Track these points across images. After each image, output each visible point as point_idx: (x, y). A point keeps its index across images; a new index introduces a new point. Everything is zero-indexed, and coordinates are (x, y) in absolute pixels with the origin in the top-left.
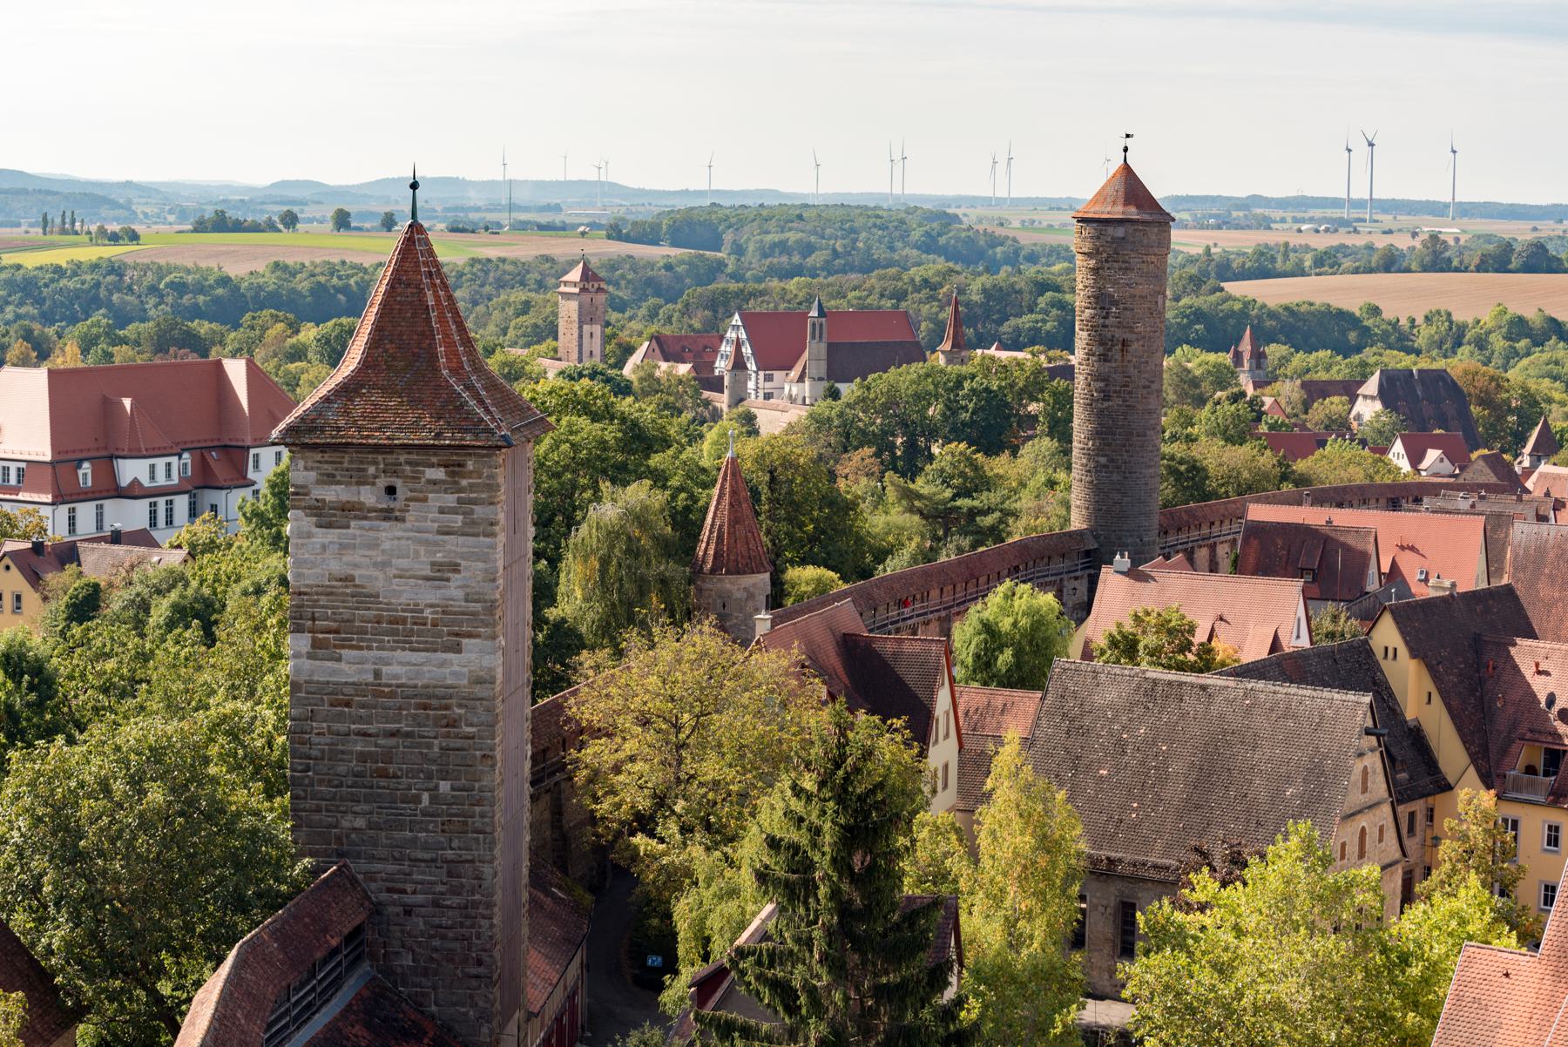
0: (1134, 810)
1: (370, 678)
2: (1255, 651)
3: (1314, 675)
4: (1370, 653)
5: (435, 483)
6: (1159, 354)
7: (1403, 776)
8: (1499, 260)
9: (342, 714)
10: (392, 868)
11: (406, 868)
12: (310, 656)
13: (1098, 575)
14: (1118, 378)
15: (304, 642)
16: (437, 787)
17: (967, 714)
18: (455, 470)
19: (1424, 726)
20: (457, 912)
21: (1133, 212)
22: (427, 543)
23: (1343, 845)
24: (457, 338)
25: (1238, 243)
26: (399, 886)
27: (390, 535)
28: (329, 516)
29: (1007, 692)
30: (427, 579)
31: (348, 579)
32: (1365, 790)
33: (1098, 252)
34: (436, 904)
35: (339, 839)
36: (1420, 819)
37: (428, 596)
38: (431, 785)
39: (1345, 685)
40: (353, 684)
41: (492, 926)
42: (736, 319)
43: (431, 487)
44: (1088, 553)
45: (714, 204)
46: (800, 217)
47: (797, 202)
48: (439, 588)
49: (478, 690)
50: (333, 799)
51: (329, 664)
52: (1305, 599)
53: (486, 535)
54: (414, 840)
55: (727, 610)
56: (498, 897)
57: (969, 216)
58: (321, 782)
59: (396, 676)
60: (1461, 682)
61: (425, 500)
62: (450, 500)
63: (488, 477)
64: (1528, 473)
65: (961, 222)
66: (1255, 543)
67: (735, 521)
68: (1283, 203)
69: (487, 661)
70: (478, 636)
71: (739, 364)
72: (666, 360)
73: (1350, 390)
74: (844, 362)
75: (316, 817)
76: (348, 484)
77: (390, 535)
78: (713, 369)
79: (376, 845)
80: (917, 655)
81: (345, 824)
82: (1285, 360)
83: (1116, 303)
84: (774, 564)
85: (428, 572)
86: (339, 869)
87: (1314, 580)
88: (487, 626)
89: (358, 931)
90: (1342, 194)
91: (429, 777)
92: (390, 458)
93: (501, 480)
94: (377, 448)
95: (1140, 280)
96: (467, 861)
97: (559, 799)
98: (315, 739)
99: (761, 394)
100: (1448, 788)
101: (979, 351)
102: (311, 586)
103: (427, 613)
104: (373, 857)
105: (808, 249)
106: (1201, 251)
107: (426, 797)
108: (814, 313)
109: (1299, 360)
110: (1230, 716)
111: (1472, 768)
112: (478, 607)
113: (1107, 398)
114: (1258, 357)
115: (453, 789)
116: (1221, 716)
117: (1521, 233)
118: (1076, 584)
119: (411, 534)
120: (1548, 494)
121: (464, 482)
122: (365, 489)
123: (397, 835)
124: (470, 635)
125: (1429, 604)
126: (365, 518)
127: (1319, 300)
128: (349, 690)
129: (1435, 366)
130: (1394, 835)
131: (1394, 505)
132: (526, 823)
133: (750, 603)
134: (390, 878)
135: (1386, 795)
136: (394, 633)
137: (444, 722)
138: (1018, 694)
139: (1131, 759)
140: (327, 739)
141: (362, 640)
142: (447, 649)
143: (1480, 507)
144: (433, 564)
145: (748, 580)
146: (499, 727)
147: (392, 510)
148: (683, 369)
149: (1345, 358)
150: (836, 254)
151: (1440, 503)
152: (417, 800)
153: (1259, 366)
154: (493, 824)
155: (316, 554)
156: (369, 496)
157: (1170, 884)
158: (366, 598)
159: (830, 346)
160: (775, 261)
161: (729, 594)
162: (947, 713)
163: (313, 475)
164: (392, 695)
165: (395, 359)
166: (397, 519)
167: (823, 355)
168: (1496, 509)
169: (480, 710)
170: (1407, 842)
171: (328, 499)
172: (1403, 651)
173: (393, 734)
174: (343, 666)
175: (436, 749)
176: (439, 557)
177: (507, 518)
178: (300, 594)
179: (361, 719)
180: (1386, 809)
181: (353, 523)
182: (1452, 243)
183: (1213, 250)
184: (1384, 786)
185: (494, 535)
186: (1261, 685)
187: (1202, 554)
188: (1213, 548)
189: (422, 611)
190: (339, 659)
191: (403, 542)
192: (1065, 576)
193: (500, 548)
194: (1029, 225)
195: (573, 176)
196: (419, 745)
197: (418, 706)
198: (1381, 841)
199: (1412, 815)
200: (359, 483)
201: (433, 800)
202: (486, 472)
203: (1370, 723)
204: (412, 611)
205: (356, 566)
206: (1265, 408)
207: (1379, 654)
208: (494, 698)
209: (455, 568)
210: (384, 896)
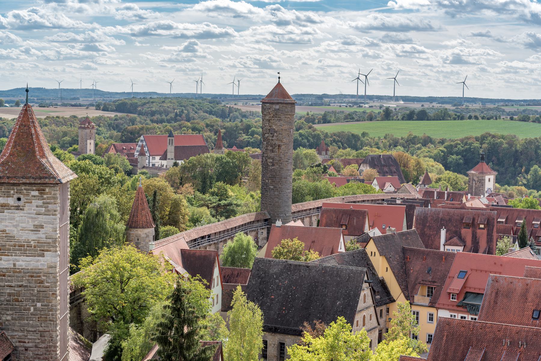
0: (284, 310)
1: (12, 266)
3: (347, 262)
7: (378, 297)
8: (410, 116)
10: (20, 334)
11: (25, 334)
13: (270, 228)
14: (277, 158)
16: (36, 305)
17: (224, 277)
18: (42, 192)
22: (32, 218)
25: (318, 111)
26: (23, 340)
27: (19, 215)
30: (32, 231)
32: (365, 302)
33: (270, 114)
36: (384, 312)
37: (32, 237)
38: (34, 304)
40: (6, 268)
41: (57, 354)
43: (33, 198)
44: (266, 220)
49: (51, 271)
53: (53, 215)
54: (28, 324)
55: (139, 241)
59: (21, 266)
61: (31, 203)
62: (40, 202)
63: (54, 194)
69: (53, 260)
70: (50, 251)
71: (142, 154)
74: (181, 152)
76: (4, 197)
77: (19, 215)
81: (4, 318)
83: (276, 132)
85: (32, 228)
88: (54, 247)
89: (9, 356)
91: (33, 301)
92: (19, 188)
93: (58, 196)
94: (14, 184)
95: (285, 124)
96: (47, 331)
97: (80, 309)
100: (394, 301)
103: (32, 243)
104: (14, 330)
105: (167, 113)
107: (32, 308)
109: (341, 151)
112: (50, 241)
113: (273, 165)
115: (42, 306)
116: (314, 276)
118: (263, 231)
119: (26, 215)
121: (45, 196)
123: (22, 322)
124: (47, 251)
126: (10, 209)
128: (4, 271)
130: (375, 318)
132: (68, 317)
133: (147, 239)
134: (20, 337)
135: (372, 303)
136: (20, 250)
137: (39, 282)
141: (9, 253)
142: (39, 256)
144: (34, 225)
145: (146, 231)
147: (19, 206)
152: (29, 309)
156: (11, 201)
158: (10, 238)
159: (175, 147)
161: (140, 235)
164: (20, 272)
165: (20, 152)
166: (21, 209)
167: (173, 150)
169: (51, 277)
170: (380, 320)
172: (377, 254)
173: (20, 286)
175: (36, 292)
176: (36, 223)
177: (60, 209)
179: (9, 281)
180: (372, 309)
181: (5, 211)
182: (394, 111)
184: (372, 300)
185: (56, 215)
188: (310, 217)
189: (30, 242)
191: (23, 218)
192: (259, 228)
195: (84, 87)
197: (29, 276)
198: (370, 320)
199: (381, 311)
200: (7, 197)
201: (35, 309)
202: (53, 192)
204: (26, 242)
205: (7, 226)
207: (369, 254)
208: (56, 273)
209: (42, 227)
210: (18, 344)
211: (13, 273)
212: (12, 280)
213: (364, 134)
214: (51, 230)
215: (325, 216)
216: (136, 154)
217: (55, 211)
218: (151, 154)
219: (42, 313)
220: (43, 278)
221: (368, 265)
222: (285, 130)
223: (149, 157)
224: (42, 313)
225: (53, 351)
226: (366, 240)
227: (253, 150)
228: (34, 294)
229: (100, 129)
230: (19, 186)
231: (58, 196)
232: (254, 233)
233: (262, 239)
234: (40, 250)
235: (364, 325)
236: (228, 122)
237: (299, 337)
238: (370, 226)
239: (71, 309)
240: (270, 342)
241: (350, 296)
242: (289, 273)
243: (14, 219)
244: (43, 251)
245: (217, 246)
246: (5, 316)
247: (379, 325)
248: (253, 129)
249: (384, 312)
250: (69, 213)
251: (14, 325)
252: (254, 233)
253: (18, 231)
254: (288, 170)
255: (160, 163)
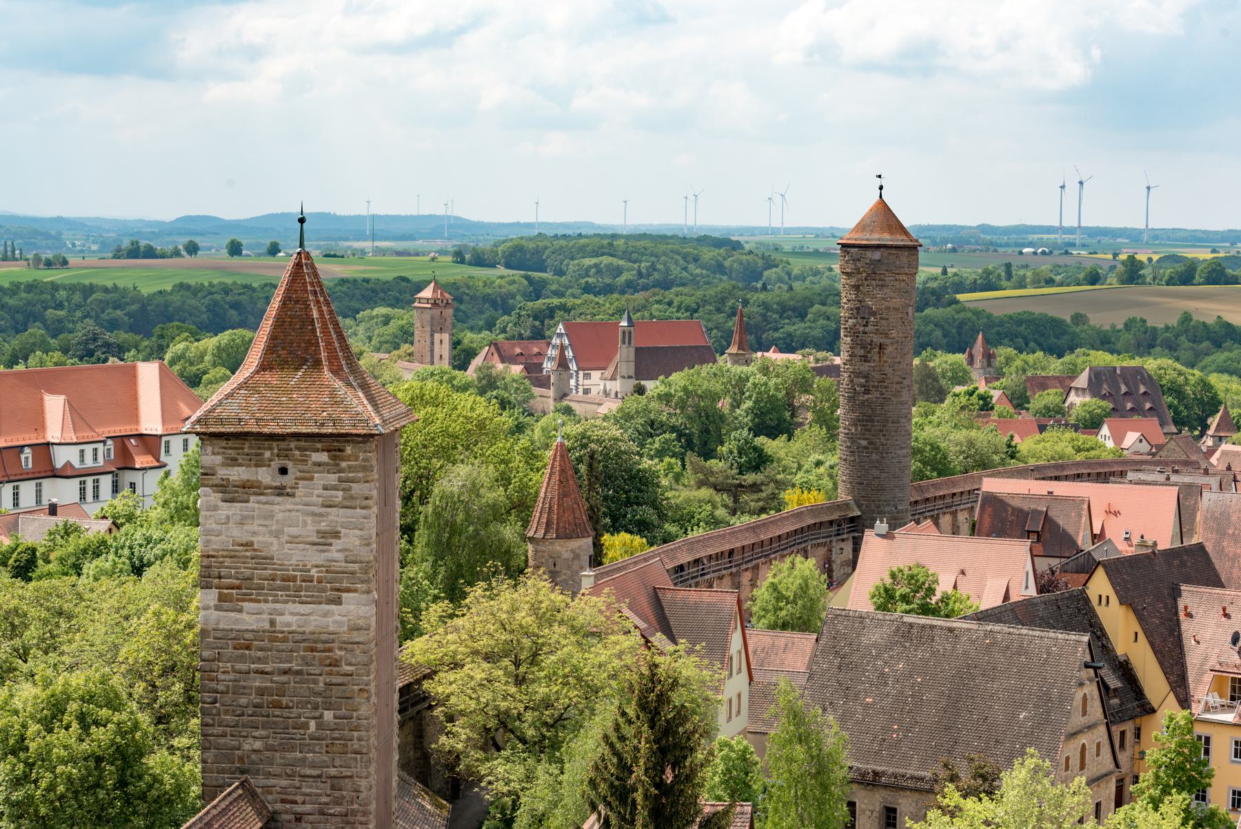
1: (267, 626)
2: (991, 599)
3: (1042, 618)
4: (1087, 600)
5: (319, 464)
6: (910, 355)
7: (1115, 701)
9: (243, 656)
10: (284, 783)
12: (217, 608)
14: (877, 376)
15: (212, 596)
16: (321, 716)
19: (1132, 661)
20: (339, 819)
21: (887, 238)
22: (314, 514)
23: (1067, 759)
24: (337, 345)
26: (290, 797)
27: (282, 508)
28: (232, 492)
29: (787, 634)
30: (314, 544)
31: (248, 544)
32: (1084, 713)
33: (859, 273)
34: (322, 813)
35: (241, 759)
36: (1129, 736)
37: (314, 557)
38: (317, 714)
39: (1067, 627)
40: (253, 631)
42: (561, 328)
43: (317, 468)
44: (852, 520)
45: (540, 234)
46: (611, 244)
47: (609, 233)
48: (324, 551)
49: (357, 637)
50: (236, 726)
51: (233, 614)
52: (1033, 556)
53: (362, 508)
54: (304, 760)
55: (557, 568)
56: (373, 807)
57: (749, 242)
58: (226, 713)
59: (288, 625)
60: (1163, 623)
61: (312, 479)
62: (332, 479)
63: (364, 460)
64: (1211, 451)
65: (743, 248)
66: (989, 510)
67: (563, 495)
68: (1007, 231)
70: (355, 591)
71: (563, 364)
72: (503, 362)
73: (1065, 382)
74: (649, 362)
75: (222, 741)
76: (249, 466)
77: (282, 508)
78: (541, 370)
79: (272, 764)
80: (714, 604)
81: (247, 747)
82: (1009, 360)
83: (874, 314)
84: (595, 529)
86: (242, 784)
87: (1039, 540)
88: (363, 582)
90: (1057, 224)
92: (283, 445)
95: (892, 294)
96: (346, 777)
97: (421, 725)
98: (221, 677)
99: (581, 390)
100: (1153, 711)
101: (759, 354)
102: (218, 551)
103: (314, 572)
104: (269, 773)
106: (939, 270)
107: (312, 724)
108: (624, 323)
110: (972, 653)
111: (1172, 694)
112: (356, 567)
113: (867, 392)
114: (989, 357)
115: (335, 717)
117: (1204, 255)
119: (300, 507)
120: (1229, 468)
121: (344, 464)
122: (262, 470)
123: (290, 755)
124: (348, 590)
125: (1133, 561)
127: (1037, 310)
128: (247, 635)
129: (1136, 362)
130: (1109, 750)
131: (1103, 478)
132: (395, 745)
133: (576, 562)
135: (1102, 717)
136: (286, 589)
137: (328, 661)
138: (797, 636)
139: (891, 689)
140: (232, 676)
141: (259, 594)
143: (1174, 478)
145: (574, 544)
146: (373, 666)
147: (284, 488)
148: (517, 370)
149: (1060, 357)
150: (640, 274)
151: (1142, 476)
152: (305, 726)
153: (989, 365)
154: (369, 747)
155: (224, 523)
156: (265, 476)
157: (926, 790)
158: (264, 560)
159: (638, 350)
160: (590, 280)
162: (740, 652)
163: (219, 459)
164: (285, 640)
166: (288, 495)
168: (1187, 480)
169: (358, 652)
170: (1119, 756)
171: (231, 478)
172: (1114, 600)
173: (285, 673)
174: (244, 616)
175: (321, 685)
176: (323, 526)
177: (379, 493)
178: (208, 556)
180: (1102, 729)
181: (252, 498)
183: (949, 270)
184: (1101, 710)
186: (997, 627)
187: (946, 520)
188: (954, 514)
189: (309, 571)
190: (240, 611)
191: (293, 513)
192: (834, 539)
193: (374, 520)
194: (800, 253)
195: (425, 211)
196: (308, 681)
198: (1098, 755)
199: (1123, 733)
200: (257, 466)
202: (362, 456)
203: (1088, 658)
205: (254, 533)
206: (994, 401)
207: (1094, 601)
209: (336, 535)
210: (278, 806)
211: (270, 641)
212: (267, 657)
213: (1079, 319)
214: (357, 542)
215: (989, 510)
216: (548, 366)
217: (367, 499)
218: (581, 365)
219: (336, 734)
220: (339, 653)
221: (1091, 626)
222: (896, 309)
223: (577, 372)
224: (336, 734)
225: (361, 823)
226: (1088, 567)
227: (821, 355)
228: (317, 689)
229: (462, 307)
230: (284, 440)
231: (374, 462)
232: (822, 551)
233: (842, 565)
234: (332, 589)
235: (1082, 767)
236: (756, 290)
237: (931, 796)
238: (1094, 536)
239: (402, 725)
240: (863, 806)
241: (1050, 700)
242: (907, 644)
243: (273, 516)
244: (338, 590)
245: (736, 579)
246: (250, 740)
247: (1117, 766)
248: (817, 307)
249: (1129, 736)
250: (399, 503)
251: (271, 762)
252: (822, 551)
253: (280, 544)
254: (902, 403)
255: (602, 387)
